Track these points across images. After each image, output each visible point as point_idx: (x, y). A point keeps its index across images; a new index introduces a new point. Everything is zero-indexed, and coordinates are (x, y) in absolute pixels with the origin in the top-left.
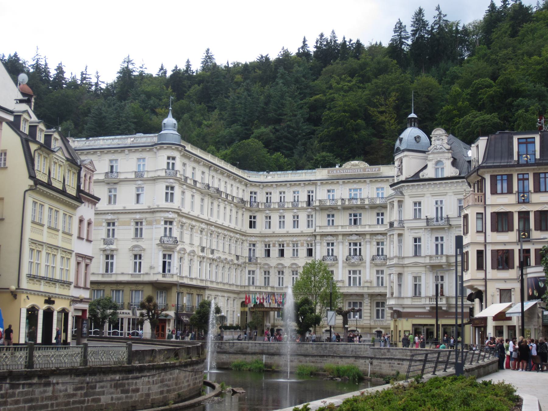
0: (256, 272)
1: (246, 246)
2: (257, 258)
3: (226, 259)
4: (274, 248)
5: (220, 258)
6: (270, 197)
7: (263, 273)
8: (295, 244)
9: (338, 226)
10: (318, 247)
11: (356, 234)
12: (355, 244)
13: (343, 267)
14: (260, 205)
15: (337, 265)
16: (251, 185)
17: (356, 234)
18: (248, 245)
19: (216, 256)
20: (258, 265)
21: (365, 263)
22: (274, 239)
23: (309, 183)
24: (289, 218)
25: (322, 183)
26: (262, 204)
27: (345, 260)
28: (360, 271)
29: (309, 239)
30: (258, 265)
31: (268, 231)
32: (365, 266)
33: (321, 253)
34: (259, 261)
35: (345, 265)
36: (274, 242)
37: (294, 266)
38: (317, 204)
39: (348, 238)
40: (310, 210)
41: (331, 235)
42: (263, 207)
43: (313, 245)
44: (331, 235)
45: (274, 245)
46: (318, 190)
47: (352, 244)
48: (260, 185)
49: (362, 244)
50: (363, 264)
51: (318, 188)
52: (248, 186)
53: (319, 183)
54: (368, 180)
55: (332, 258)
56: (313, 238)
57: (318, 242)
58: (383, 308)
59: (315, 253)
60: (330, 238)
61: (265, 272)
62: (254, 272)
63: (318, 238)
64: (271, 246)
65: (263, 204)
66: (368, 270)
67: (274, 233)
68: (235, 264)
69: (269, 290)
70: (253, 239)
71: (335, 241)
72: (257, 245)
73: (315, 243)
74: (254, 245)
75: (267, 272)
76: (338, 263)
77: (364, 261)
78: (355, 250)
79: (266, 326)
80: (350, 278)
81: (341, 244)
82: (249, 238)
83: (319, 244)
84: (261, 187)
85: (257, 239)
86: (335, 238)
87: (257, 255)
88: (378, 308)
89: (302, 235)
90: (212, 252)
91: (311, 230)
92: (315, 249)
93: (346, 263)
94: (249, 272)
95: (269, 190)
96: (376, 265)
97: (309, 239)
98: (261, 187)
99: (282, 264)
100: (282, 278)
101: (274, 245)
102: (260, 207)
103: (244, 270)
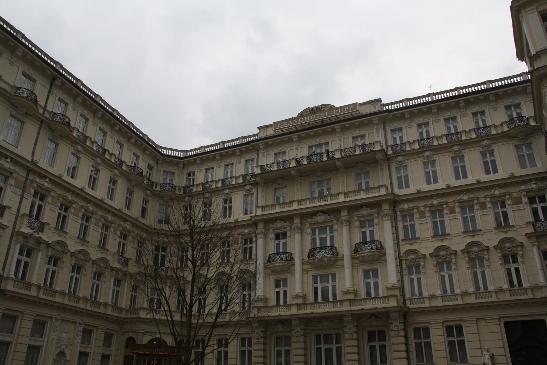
6: (194, 179)
8: (226, 243)
10: (261, 241)
11: (324, 212)
12: (322, 230)
13: (304, 271)
14: (177, 189)
15: (292, 268)
16: (165, 161)
17: (324, 212)
19: (48, 236)
21: (342, 259)
23: (247, 148)
24: (217, 204)
26: (180, 189)
27: (306, 259)
28: (334, 276)
29: (246, 231)
32: (343, 266)
33: (265, 250)
35: (307, 266)
39: (309, 220)
40: (248, 187)
42: (182, 192)
43: (254, 239)
46: (260, 156)
47: (317, 231)
49: (335, 227)
50: (340, 263)
51: (261, 152)
52: (160, 162)
53: (261, 144)
54: (337, 126)
55: (283, 256)
57: (261, 233)
58: (382, 343)
60: (279, 225)
63: (261, 226)
65: (182, 189)
66: (347, 271)
68: (113, 269)
71: (288, 228)
73: (256, 236)
74: (164, 249)
76: (294, 265)
77: (341, 255)
78: (323, 240)
80: (316, 289)
81: (298, 231)
82: (155, 238)
83: (262, 236)
86: (287, 223)
88: (373, 344)
89: (237, 225)
90: (42, 227)
91: (247, 217)
92: (257, 245)
93: (307, 262)
95: (191, 169)
96: (363, 261)
97: (246, 231)
98: (181, 166)
102: (177, 192)
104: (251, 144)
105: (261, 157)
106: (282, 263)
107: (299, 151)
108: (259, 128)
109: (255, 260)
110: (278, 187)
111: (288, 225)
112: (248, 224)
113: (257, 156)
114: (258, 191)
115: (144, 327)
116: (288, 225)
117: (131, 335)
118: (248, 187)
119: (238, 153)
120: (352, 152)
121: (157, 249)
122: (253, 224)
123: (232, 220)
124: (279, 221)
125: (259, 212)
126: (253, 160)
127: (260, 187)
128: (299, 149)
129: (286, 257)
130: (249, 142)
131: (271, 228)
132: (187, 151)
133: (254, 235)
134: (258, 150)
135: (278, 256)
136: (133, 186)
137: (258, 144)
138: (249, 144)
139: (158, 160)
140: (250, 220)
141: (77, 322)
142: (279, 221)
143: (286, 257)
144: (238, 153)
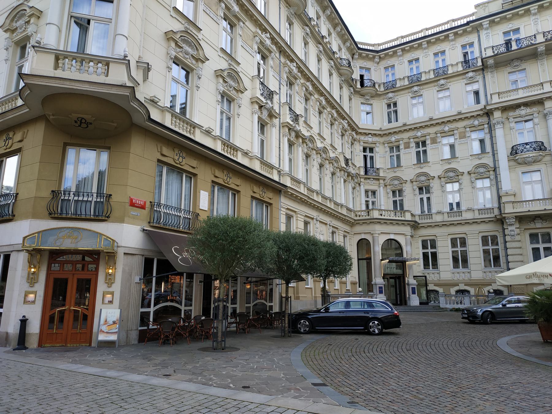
0: (377, 194)
1: (359, 148)
2: (378, 169)
3: (325, 150)
4: (407, 150)
5: (312, 139)
7: (391, 194)
9: (542, 84)
10: (499, 132)
18: (362, 148)
20: (381, 181)
22: (406, 135)
25: (493, 23)
30: (381, 181)
31: (394, 124)
34: (382, 174)
36: (405, 141)
37: (451, 174)
38: (490, 53)
41: (526, 105)
42: (382, 89)
44: (526, 105)
45: (407, 146)
48: (374, 57)
51: (483, 34)
52: (356, 56)
53: (485, 22)
56: (485, 120)
57: (498, 123)
59: (492, 145)
61: (394, 192)
62: (374, 193)
63: (497, 115)
64: (402, 147)
65: (382, 86)
67: (405, 125)
69: (408, 217)
70: (370, 139)
72: (376, 149)
74: (371, 150)
75: (398, 192)
79: (408, 285)
82: (362, 138)
84: (377, 60)
85: (375, 139)
87: (378, 165)
94: (367, 192)
97: (476, 123)
98: (377, 60)
99: (425, 174)
100: (428, 199)
101: (407, 146)
103: (358, 188)
104: (470, 25)
105: (485, 38)
106: (536, 153)
107: (491, 39)
108: (477, 6)
109: (491, 154)
110: (515, 70)
111: (536, 111)
112: (478, 115)
113: (477, 38)
114: (485, 77)
115: (378, 228)
116: (536, 111)
117: (363, 236)
118: (471, 74)
119: (451, 37)
120: (531, 41)
121: (365, 150)
122: (483, 114)
123: (400, 123)
124: (522, 108)
125: (496, 99)
126: (471, 45)
127: (489, 73)
128: (539, 23)
129: (540, 147)
130: (468, 23)
131: (512, 116)
132: (379, 45)
133: (486, 126)
134: (478, 31)
135: (528, 147)
136: (342, 80)
137: (481, 23)
138: (469, 25)
139: (353, 54)
140: (481, 110)
141: (328, 223)
142: (522, 108)
143: (540, 147)
144: (451, 37)
